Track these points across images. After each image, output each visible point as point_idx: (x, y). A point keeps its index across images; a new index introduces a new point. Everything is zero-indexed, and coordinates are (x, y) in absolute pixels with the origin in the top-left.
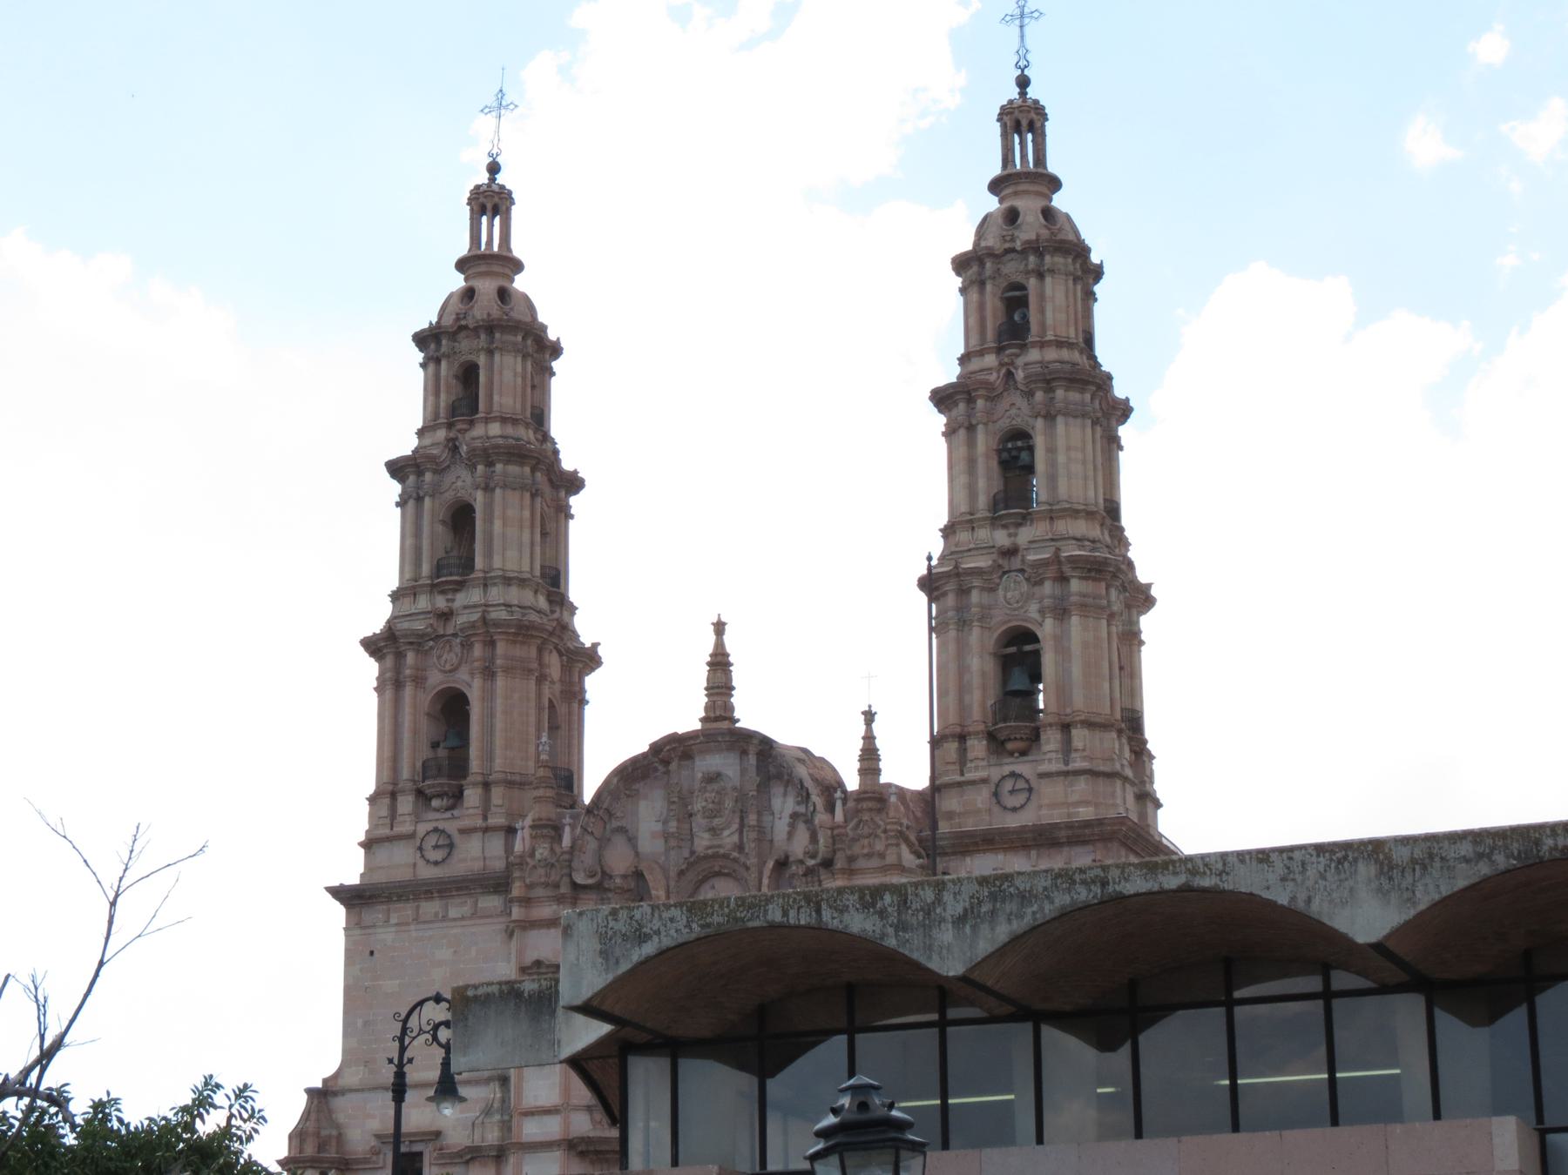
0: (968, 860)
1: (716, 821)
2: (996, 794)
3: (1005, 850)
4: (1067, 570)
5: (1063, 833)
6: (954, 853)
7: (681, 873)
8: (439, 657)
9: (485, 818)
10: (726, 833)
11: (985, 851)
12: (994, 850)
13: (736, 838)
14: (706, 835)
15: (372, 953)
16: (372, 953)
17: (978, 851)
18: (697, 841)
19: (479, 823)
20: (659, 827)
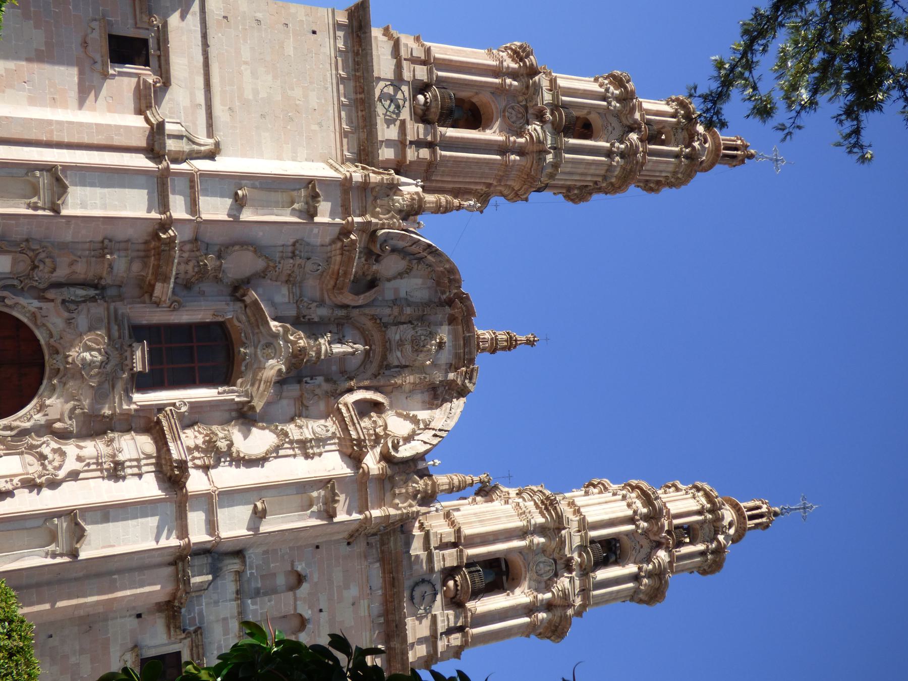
0: (378, 565)
1: (408, 347)
2: (423, 581)
3: (385, 595)
4: (558, 612)
5: (395, 644)
6: (382, 552)
7: (373, 318)
8: (513, 108)
9: (411, 143)
10: (399, 354)
11: (384, 578)
12: (384, 588)
13: (396, 363)
14: (398, 337)
15: (314, 32)
16: (314, 32)
17: (384, 572)
18: (394, 328)
19: (409, 138)
20: (403, 294)
